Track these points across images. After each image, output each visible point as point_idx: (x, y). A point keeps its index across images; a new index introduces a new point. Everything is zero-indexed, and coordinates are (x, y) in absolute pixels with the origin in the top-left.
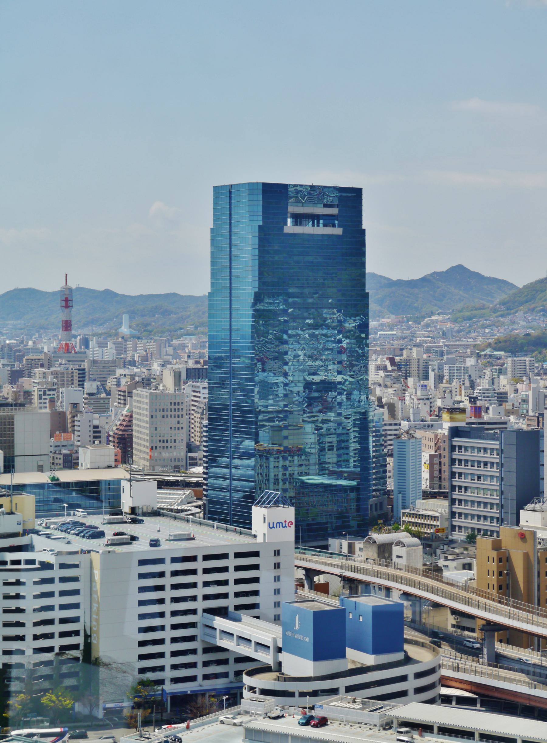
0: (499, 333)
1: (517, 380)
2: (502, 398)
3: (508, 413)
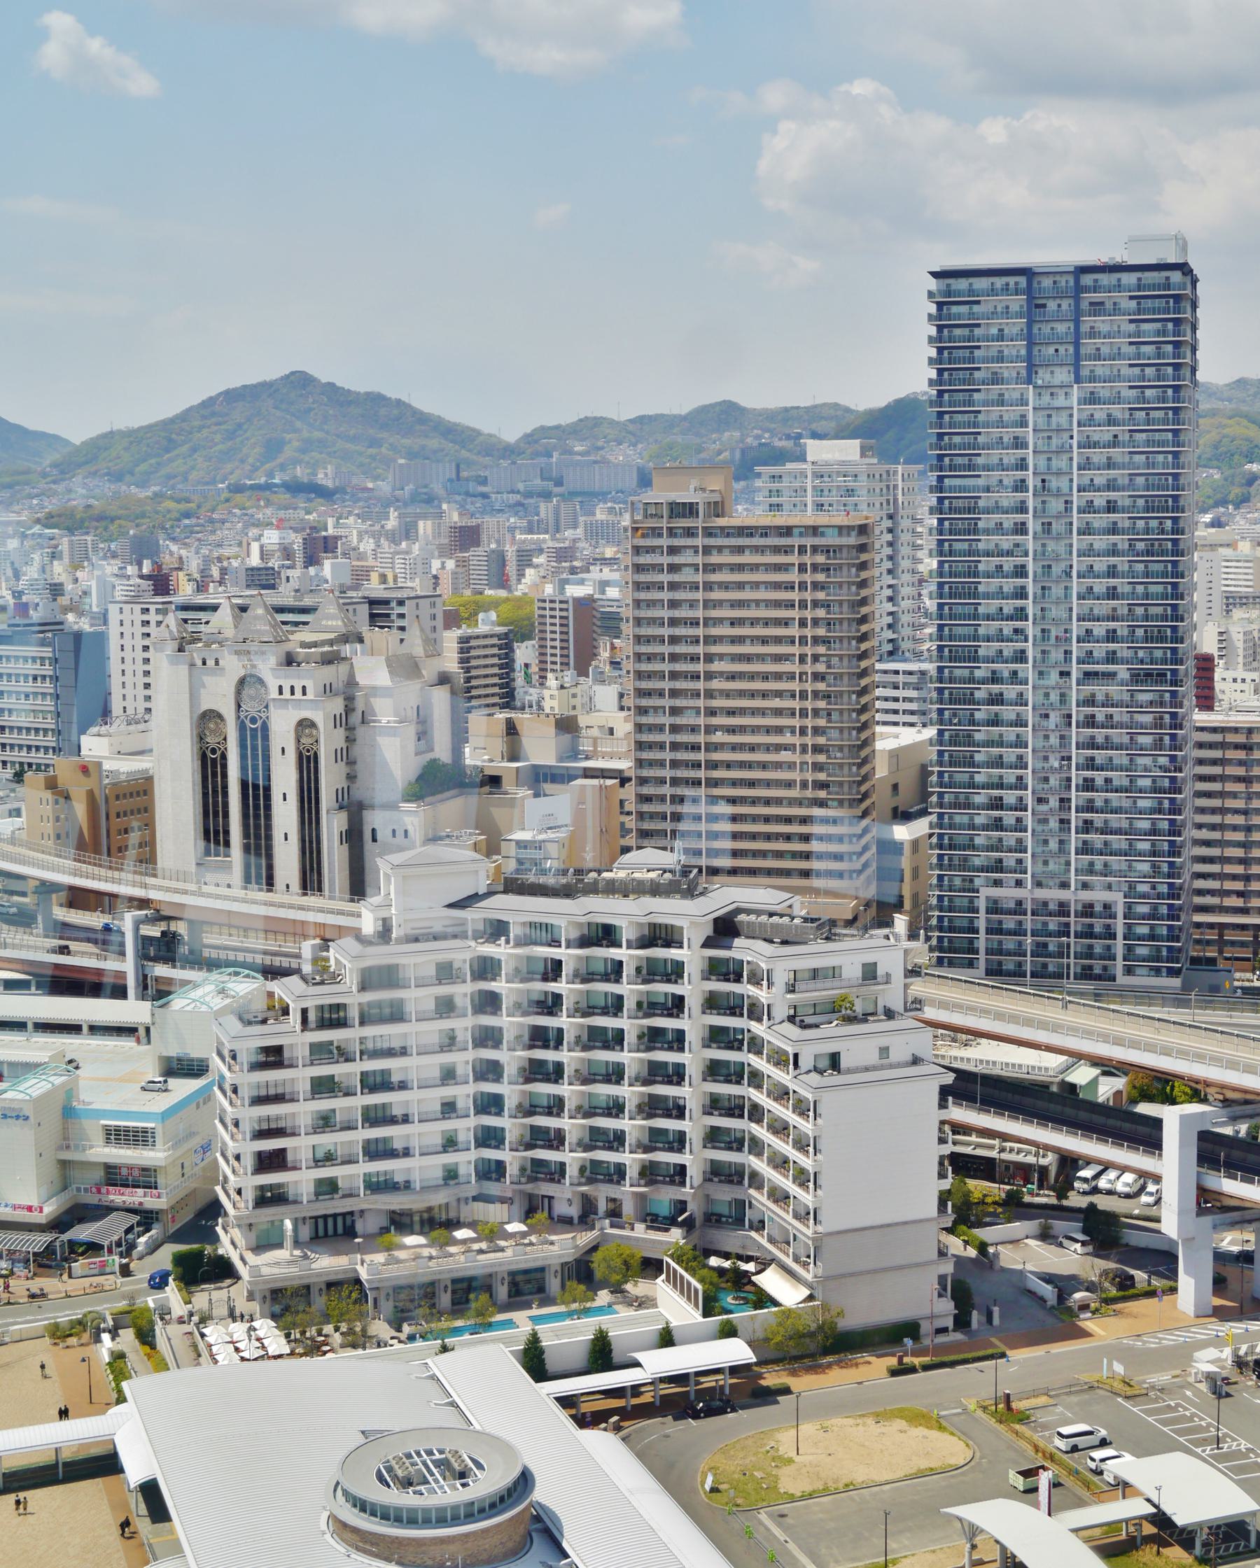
0: (51, 505)
1: (76, 566)
2: (56, 590)
3: (66, 610)
